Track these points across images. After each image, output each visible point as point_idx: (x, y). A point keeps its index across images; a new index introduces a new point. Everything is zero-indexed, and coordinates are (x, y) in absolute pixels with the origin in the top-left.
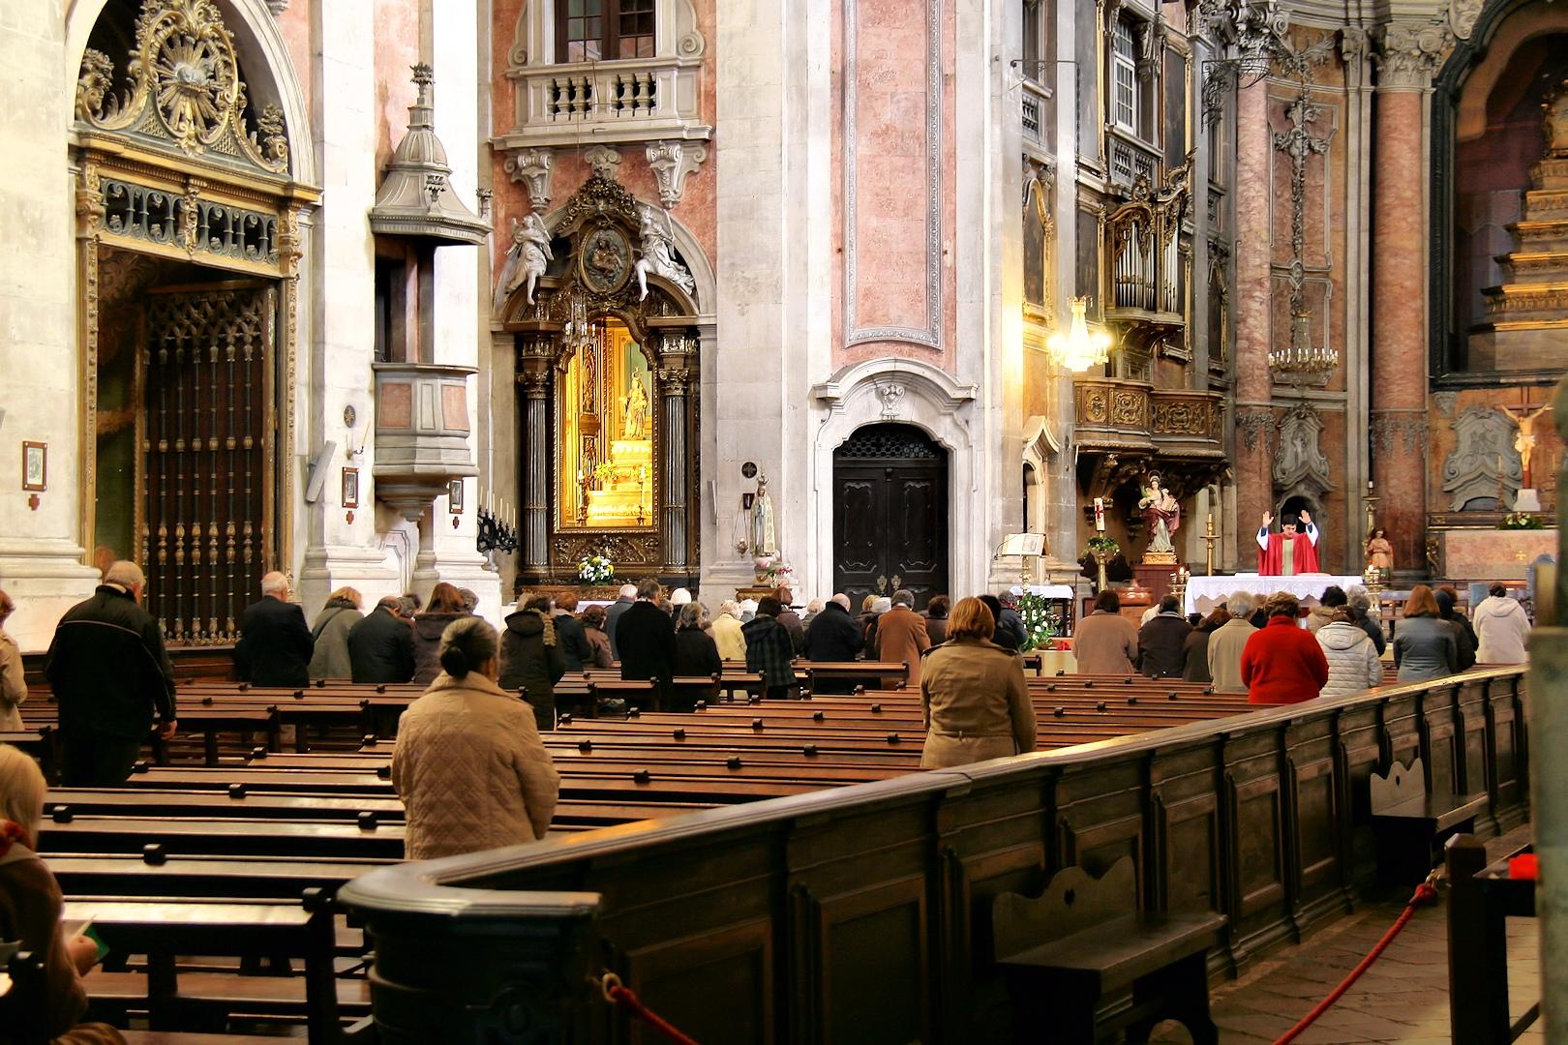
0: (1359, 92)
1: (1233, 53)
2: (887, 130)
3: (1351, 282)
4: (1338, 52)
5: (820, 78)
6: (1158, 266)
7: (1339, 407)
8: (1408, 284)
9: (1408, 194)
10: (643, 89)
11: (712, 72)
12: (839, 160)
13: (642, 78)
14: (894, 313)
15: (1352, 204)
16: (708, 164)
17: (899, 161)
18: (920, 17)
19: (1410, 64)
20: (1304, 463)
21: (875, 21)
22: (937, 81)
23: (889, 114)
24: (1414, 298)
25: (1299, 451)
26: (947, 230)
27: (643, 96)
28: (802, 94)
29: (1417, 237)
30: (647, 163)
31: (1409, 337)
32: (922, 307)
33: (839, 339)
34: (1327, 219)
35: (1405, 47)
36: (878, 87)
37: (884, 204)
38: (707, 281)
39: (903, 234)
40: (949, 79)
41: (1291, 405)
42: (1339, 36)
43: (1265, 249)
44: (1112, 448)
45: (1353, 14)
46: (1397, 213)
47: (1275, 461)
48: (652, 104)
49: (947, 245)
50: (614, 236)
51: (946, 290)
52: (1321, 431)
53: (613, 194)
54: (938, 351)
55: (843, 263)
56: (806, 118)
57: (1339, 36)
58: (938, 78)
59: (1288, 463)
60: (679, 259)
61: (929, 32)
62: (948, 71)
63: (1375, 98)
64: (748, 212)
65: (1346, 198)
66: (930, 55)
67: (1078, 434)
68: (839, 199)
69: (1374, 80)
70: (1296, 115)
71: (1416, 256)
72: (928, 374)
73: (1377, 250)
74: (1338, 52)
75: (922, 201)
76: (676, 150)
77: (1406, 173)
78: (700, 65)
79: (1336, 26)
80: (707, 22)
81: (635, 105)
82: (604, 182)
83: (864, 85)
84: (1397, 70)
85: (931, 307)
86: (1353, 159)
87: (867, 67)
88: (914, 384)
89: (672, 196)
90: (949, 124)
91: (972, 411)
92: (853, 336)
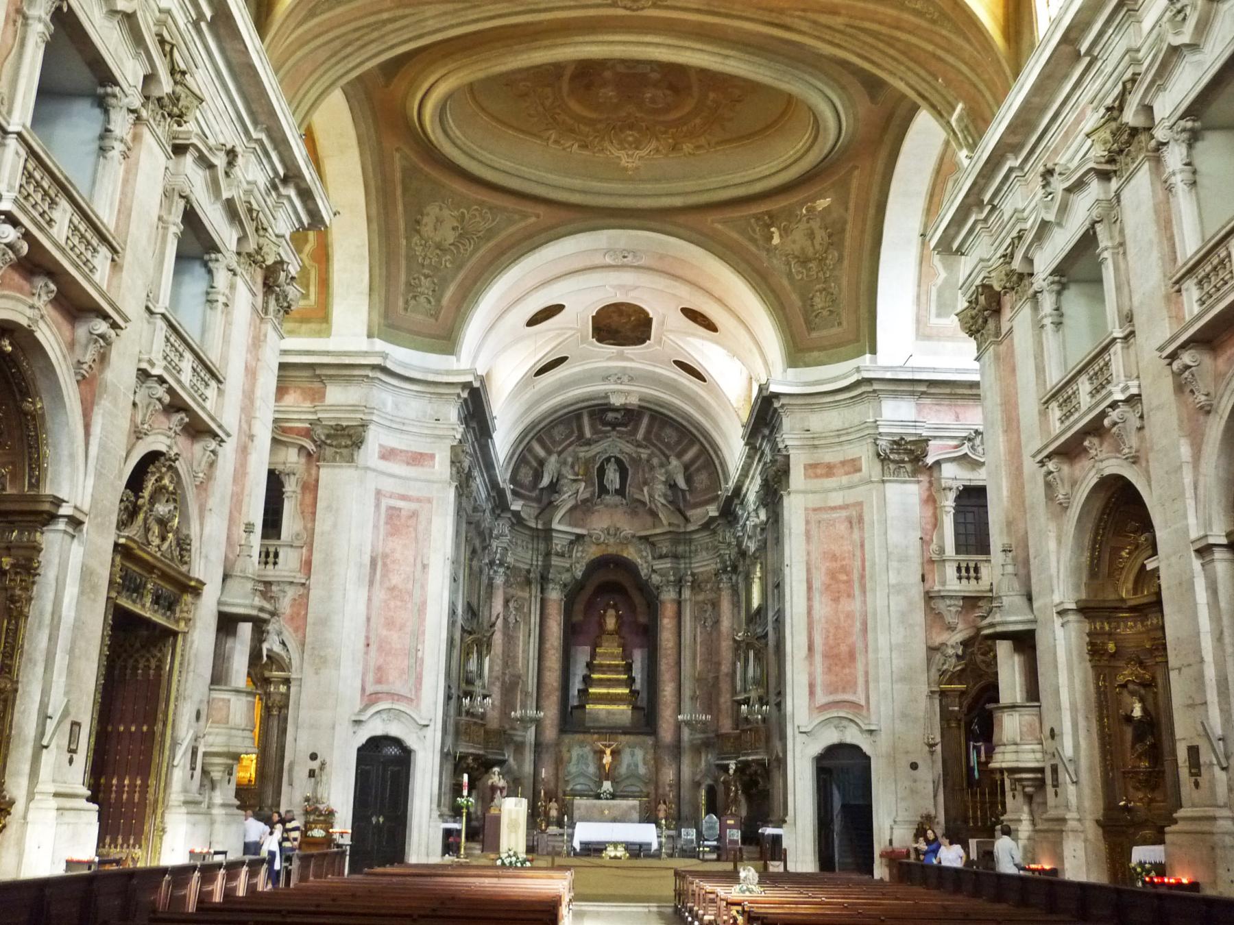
10: (272, 555)
17: (399, 603)
21: (392, 535)
22: (419, 567)
27: (271, 559)
44: (472, 754)
48: (275, 563)
49: (419, 647)
54: (412, 700)
57: (529, 571)
63: (542, 599)
64: (324, 622)
70: (511, 605)
79: (527, 567)
81: (266, 563)
83: (385, 565)
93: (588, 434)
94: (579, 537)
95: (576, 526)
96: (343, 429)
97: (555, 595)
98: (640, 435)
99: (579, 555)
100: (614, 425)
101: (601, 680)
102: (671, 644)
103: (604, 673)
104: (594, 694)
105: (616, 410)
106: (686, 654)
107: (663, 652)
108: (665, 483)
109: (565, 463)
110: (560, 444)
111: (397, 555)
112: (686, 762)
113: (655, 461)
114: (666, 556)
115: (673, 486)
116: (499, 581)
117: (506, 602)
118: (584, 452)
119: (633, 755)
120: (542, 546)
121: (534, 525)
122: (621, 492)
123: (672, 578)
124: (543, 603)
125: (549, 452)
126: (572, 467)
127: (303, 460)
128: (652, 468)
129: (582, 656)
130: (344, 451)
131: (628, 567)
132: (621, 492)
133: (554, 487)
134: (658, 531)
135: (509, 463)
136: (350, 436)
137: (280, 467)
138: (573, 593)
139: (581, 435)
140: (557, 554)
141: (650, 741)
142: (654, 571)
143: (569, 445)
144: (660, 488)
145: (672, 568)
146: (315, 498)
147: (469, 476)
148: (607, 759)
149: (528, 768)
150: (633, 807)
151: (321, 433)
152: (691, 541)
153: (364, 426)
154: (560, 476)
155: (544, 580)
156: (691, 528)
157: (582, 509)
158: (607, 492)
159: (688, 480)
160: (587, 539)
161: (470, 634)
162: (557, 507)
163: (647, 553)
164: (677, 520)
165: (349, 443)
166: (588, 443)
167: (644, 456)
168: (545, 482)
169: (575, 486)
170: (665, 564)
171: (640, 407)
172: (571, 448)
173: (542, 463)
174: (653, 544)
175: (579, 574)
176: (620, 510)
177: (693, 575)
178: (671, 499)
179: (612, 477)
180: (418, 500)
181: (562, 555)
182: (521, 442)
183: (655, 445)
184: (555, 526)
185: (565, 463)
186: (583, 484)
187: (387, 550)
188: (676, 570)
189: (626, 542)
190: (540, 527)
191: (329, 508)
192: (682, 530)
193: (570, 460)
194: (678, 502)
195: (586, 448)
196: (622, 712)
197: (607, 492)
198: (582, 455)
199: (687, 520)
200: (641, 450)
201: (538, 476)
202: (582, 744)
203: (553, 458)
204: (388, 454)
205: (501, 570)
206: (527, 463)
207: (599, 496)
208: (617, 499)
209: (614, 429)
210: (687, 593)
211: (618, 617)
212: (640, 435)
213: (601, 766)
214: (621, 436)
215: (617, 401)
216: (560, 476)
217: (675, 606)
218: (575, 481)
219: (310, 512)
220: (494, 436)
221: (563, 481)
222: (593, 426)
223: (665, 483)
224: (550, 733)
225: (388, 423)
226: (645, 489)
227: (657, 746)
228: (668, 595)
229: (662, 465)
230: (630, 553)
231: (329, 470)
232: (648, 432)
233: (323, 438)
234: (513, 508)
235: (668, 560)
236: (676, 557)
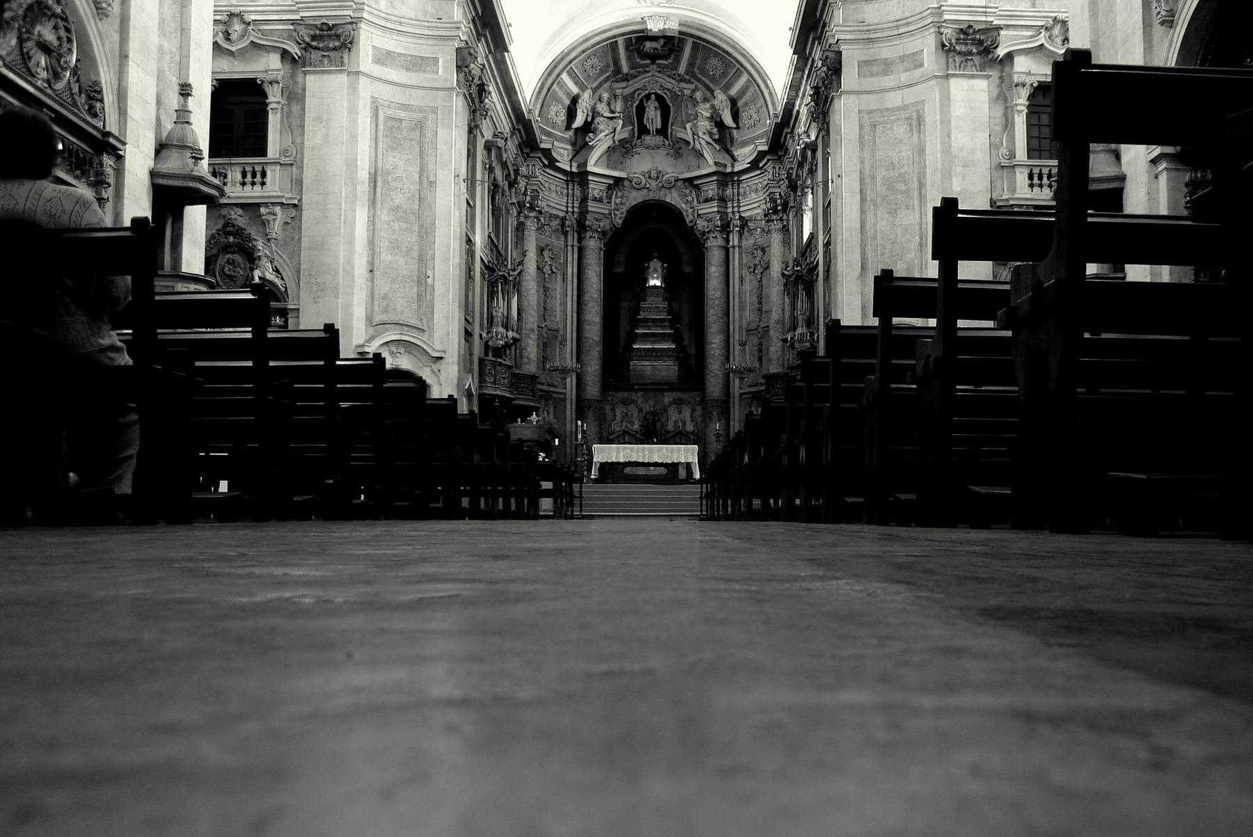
1: (522, 219)
2: (397, 209)
4: (563, 225)
5: (363, 174)
6: (509, 308)
10: (259, 176)
11: (301, 168)
12: (372, 221)
13: (258, 169)
14: (399, 308)
15: (569, 299)
16: (298, 219)
17: (404, 226)
18: (417, 149)
19: (596, 235)
21: (393, 149)
23: (398, 199)
26: (430, 264)
27: (258, 179)
28: (353, 182)
30: (260, 216)
32: (415, 306)
33: (369, 320)
35: (594, 227)
36: (393, 184)
37: (395, 247)
38: (293, 285)
39: (405, 265)
40: (432, 184)
43: (535, 314)
46: (590, 305)
48: (263, 184)
50: (238, 258)
51: (428, 298)
53: (239, 232)
55: (372, 279)
56: (355, 196)
57: (564, 219)
58: (426, 183)
60: (277, 271)
61: (422, 158)
62: (433, 179)
63: (580, 250)
66: (422, 170)
67: (480, 387)
68: (371, 243)
70: (546, 253)
72: (419, 343)
74: (563, 225)
75: (416, 248)
76: (278, 209)
78: (292, 163)
79: (562, 214)
80: (298, 141)
81: (253, 184)
82: (233, 226)
83: (386, 182)
85: (419, 306)
87: (388, 173)
88: (409, 347)
89: (274, 235)
90: (431, 207)
91: (442, 365)
92: (377, 319)
93: (625, 69)
94: (618, 181)
95: (615, 168)
96: (330, 29)
97: (594, 245)
98: (682, 69)
99: (618, 201)
100: (653, 57)
101: (645, 335)
105: (655, 38)
108: (711, 118)
109: (600, 100)
110: (595, 79)
111: (400, 172)
113: (698, 95)
114: (711, 200)
115: (720, 124)
116: (531, 226)
117: (541, 251)
118: (621, 88)
120: (578, 192)
122: (663, 132)
124: (581, 251)
125: (583, 88)
126: (609, 104)
127: (288, 67)
128: (695, 103)
130: (332, 54)
131: (670, 214)
132: (663, 132)
133: (588, 128)
135: (537, 98)
136: (338, 36)
137: (260, 76)
138: (614, 242)
139: (618, 70)
140: (595, 199)
142: (699, 216)
143: (606, 80)
144: (704, 125)
146: (303, 109)
147: (482, 89)
151: (305, 34)
152: (739, 182)
153: (354, 22)
154: (595, 113)
156: (738, 168)
157: (622, 150)
158: (647, 132)
159: (736, 116)
160: (626, 183)
161: (496, 276)
162: (593, 147)
165: (337, 44)
166: (626, 78)
167: (687, 92)
168: (579, 122)
169: (611, 123)
171: (680, 33)
172: (608, 84)
173: (575, 100)
175: (619, 221)
176: (663, 152)
177: (741, 218)
178: (717, 137)
179: (653, 115)
180: (421, 110)
181: (600, 201)
182: (549, 75)
183: (698, 80)
184: (589, 169)
185: (600, 100)
186: (621, 122)
187: (387, 166)
188: (723, 215)
189: (670, 186)
190: (574, 170)
191: (319, 119)
192: (729, 170)
193: (606, 96)
194: (724, 138)
195: (624, 84)
196: (668, 369)
197: (647, 132)
198: (619, 92)
199: (734, 159)
200: (683, 85)
201: (571, 114)
204: (384, 58)
205: (533, 214)
206: (559, 101)
207: (639, 137)
208: (659, 139)
209: (653, 63)
210: (734, 239)
212: (682, 69)
214: (662, 70)
215: (654, 27)
216: (595, 113)
217: (723, 252)
219: (295, 125)
220: (510, 48)
221: (597, 120)
222: (629, 58)
223: (711, 118)
225: (383, 23)
226: (688, 126)
228: (714, 243)
229: (705, 100)
230: (673, 198)
231: (317, 77)
232: (691, 64)
233: (307, 39)
234: (543, 146)
235: (715, 203)
236: (723, 200)
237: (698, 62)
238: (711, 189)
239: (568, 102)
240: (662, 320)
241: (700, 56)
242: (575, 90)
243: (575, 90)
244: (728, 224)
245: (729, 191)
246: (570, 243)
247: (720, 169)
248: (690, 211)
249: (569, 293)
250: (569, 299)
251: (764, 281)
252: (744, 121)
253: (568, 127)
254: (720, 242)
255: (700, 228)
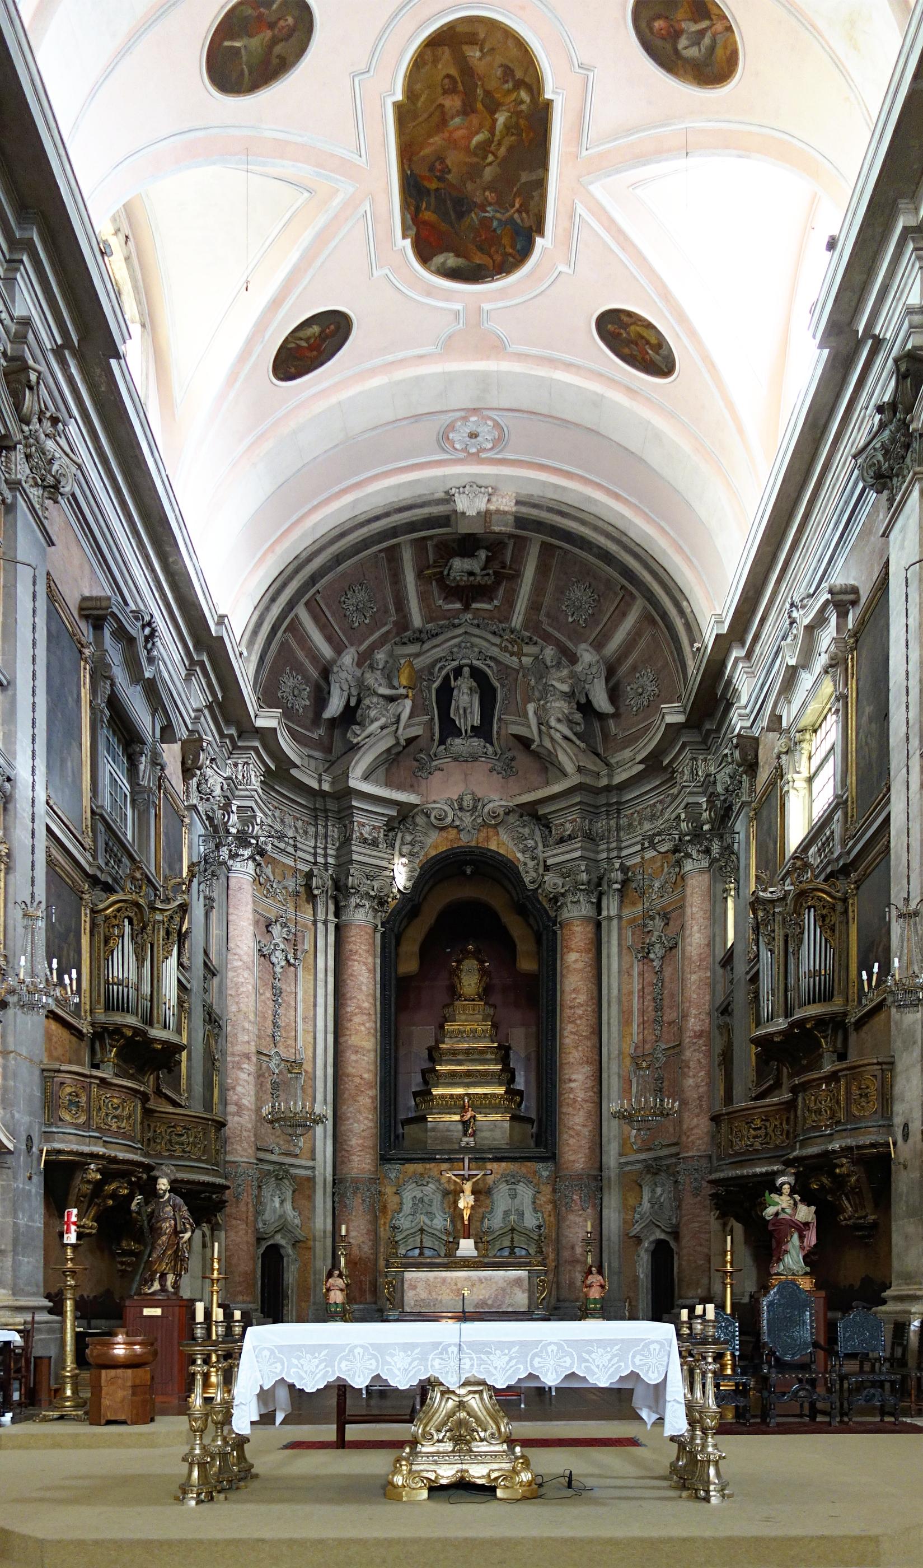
0: (325, 922)
3: (320, 1073)
4: (308, 887)
7: (308, 1173)
8: (366, 1076)
9: (366, 1005)
15: (320, 1010)
20: (280, 1216)
24: (371, 1088)
25: (278, 1205)
29: (373, 1040)
31: (367, 1118)
34: (299, 1020)
41: (270, 1168)
42: (309, 875)
45: (320, 860)
46: (357, 1019)
47: (258, 1213)
52: (294, 1191)
57: (309, 875)
59: (268, 1216)
63: (337, 927)
65: (315, 1005)
69: (337, 915)
71: (372, 1055)
73: (341, 1048)
74: (308, 887)
77: (364, 988)
79: (306, 868)
84: (357, 906)
86: (321, 975)
95: (400, 787)
97: (362, 918)
100: (468, 593)
101: (453, 1074)
102: (582, 998)
103: (460, 1063)
104: (442, 1097)
106: (611, 1015)
107: (568, 1012)
112: (612, 1202)
114: (570, 837)
115: (586, 708)
119: (513, 1196)
120: (334, 832)
121: (316, 786)
123: (584, 877)
129: (420, 1035)
133: (350, 716)
134: (556, 788)
138: (399, 919)
141: (544, 1170)
142: (547, 868)
145: (582, 858)
148: (466, 1202)
149: (322, 1222)
150: (518, 1281)
154: (363, 690)
155: (340, 892)
159: (614, 695)
163: (535, 837)
164: (591, 763)
168: (335, 707)
170: (571, 853)
174: (544, 823)
177: (624, 869)
181: (375, 843)
189: (495, 822)
202: (420, 1180)
203: (348, 658)
206: (298, 668)
210: (611, 906)
211: (483, 972)
213: (456, 1214)
216: (363, 690)
217: (590, 928)
218: (391, 699)
221: (367, 702)
222: (424, 597)
224: (361, 1161)
227: (556, 1178)
236: (590, 838)
237: (547, 600)
238: (568, 822)
239: (314, 673)
240: (482, 1051)
241: (551, 587)
242: (326, 650)
243: (326, 650)
244: (600, 879)
245: (601, 825)
246: (321, 916)
247: (588, 780)
248: (531, 864)
249: (320, 1000)
250: (320, 1010)
251: (668, 972)
252: (631, 701)
253: (317, 719)
254: (586, 909)
255: (549, 887)
